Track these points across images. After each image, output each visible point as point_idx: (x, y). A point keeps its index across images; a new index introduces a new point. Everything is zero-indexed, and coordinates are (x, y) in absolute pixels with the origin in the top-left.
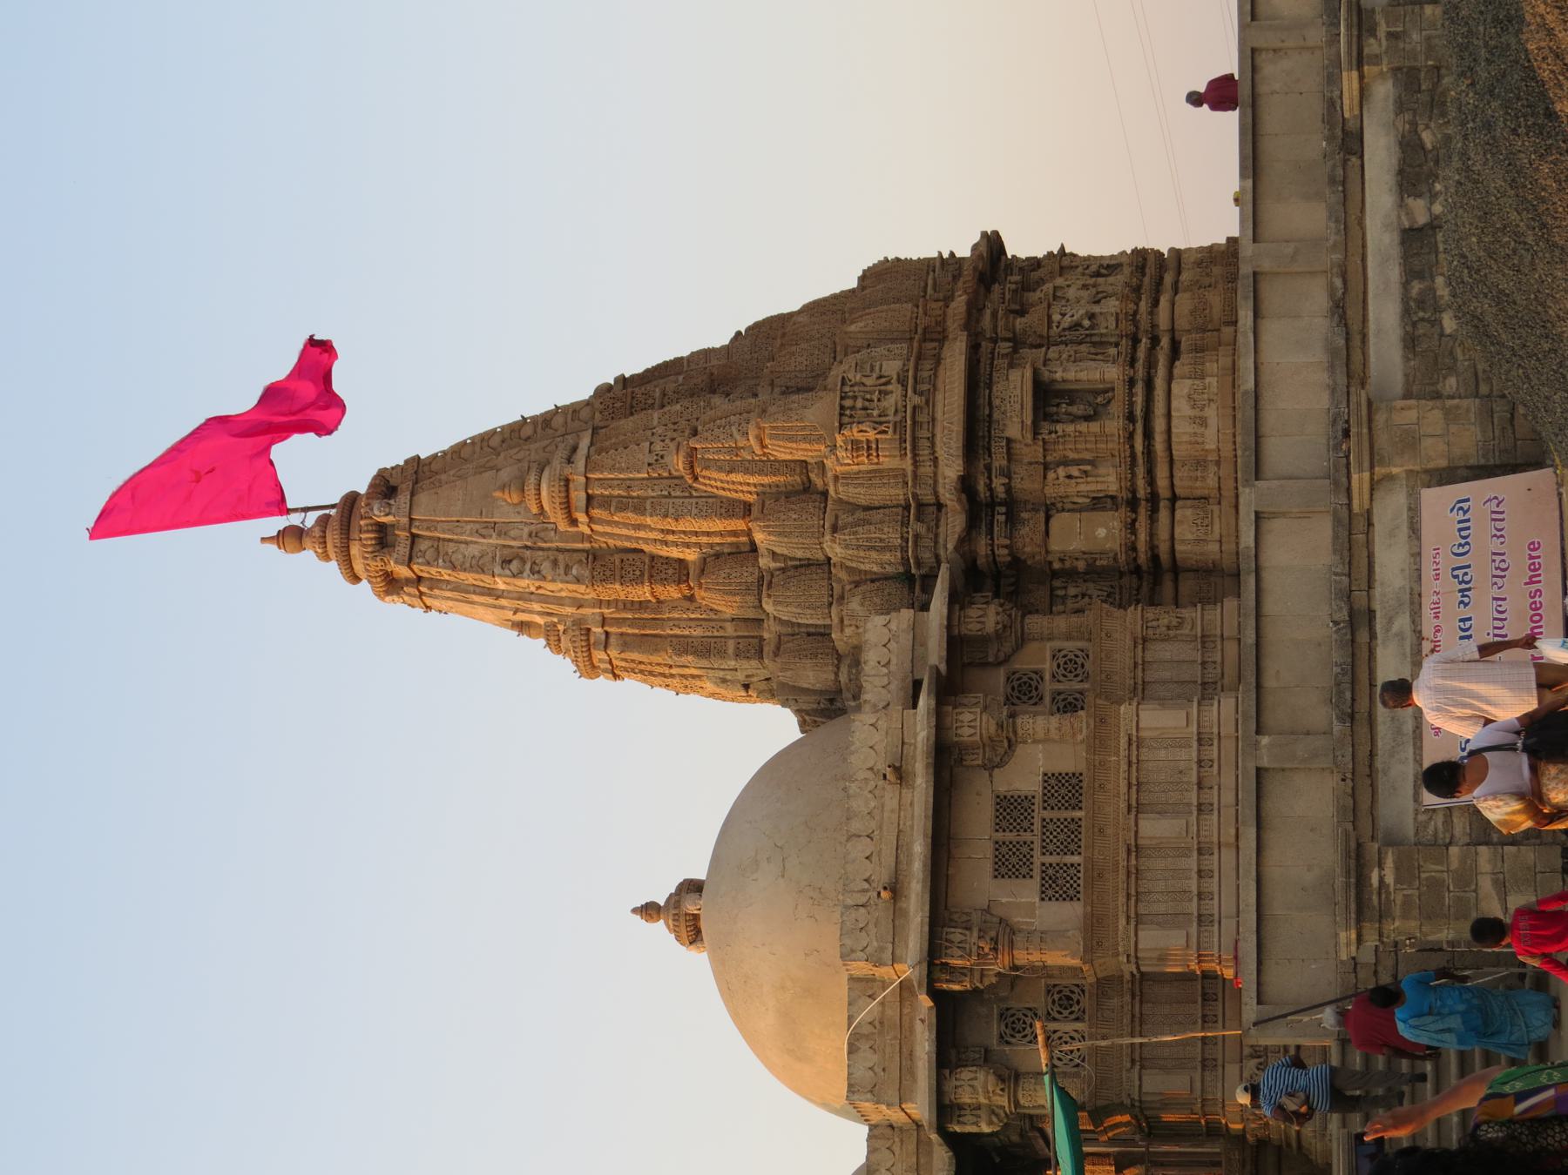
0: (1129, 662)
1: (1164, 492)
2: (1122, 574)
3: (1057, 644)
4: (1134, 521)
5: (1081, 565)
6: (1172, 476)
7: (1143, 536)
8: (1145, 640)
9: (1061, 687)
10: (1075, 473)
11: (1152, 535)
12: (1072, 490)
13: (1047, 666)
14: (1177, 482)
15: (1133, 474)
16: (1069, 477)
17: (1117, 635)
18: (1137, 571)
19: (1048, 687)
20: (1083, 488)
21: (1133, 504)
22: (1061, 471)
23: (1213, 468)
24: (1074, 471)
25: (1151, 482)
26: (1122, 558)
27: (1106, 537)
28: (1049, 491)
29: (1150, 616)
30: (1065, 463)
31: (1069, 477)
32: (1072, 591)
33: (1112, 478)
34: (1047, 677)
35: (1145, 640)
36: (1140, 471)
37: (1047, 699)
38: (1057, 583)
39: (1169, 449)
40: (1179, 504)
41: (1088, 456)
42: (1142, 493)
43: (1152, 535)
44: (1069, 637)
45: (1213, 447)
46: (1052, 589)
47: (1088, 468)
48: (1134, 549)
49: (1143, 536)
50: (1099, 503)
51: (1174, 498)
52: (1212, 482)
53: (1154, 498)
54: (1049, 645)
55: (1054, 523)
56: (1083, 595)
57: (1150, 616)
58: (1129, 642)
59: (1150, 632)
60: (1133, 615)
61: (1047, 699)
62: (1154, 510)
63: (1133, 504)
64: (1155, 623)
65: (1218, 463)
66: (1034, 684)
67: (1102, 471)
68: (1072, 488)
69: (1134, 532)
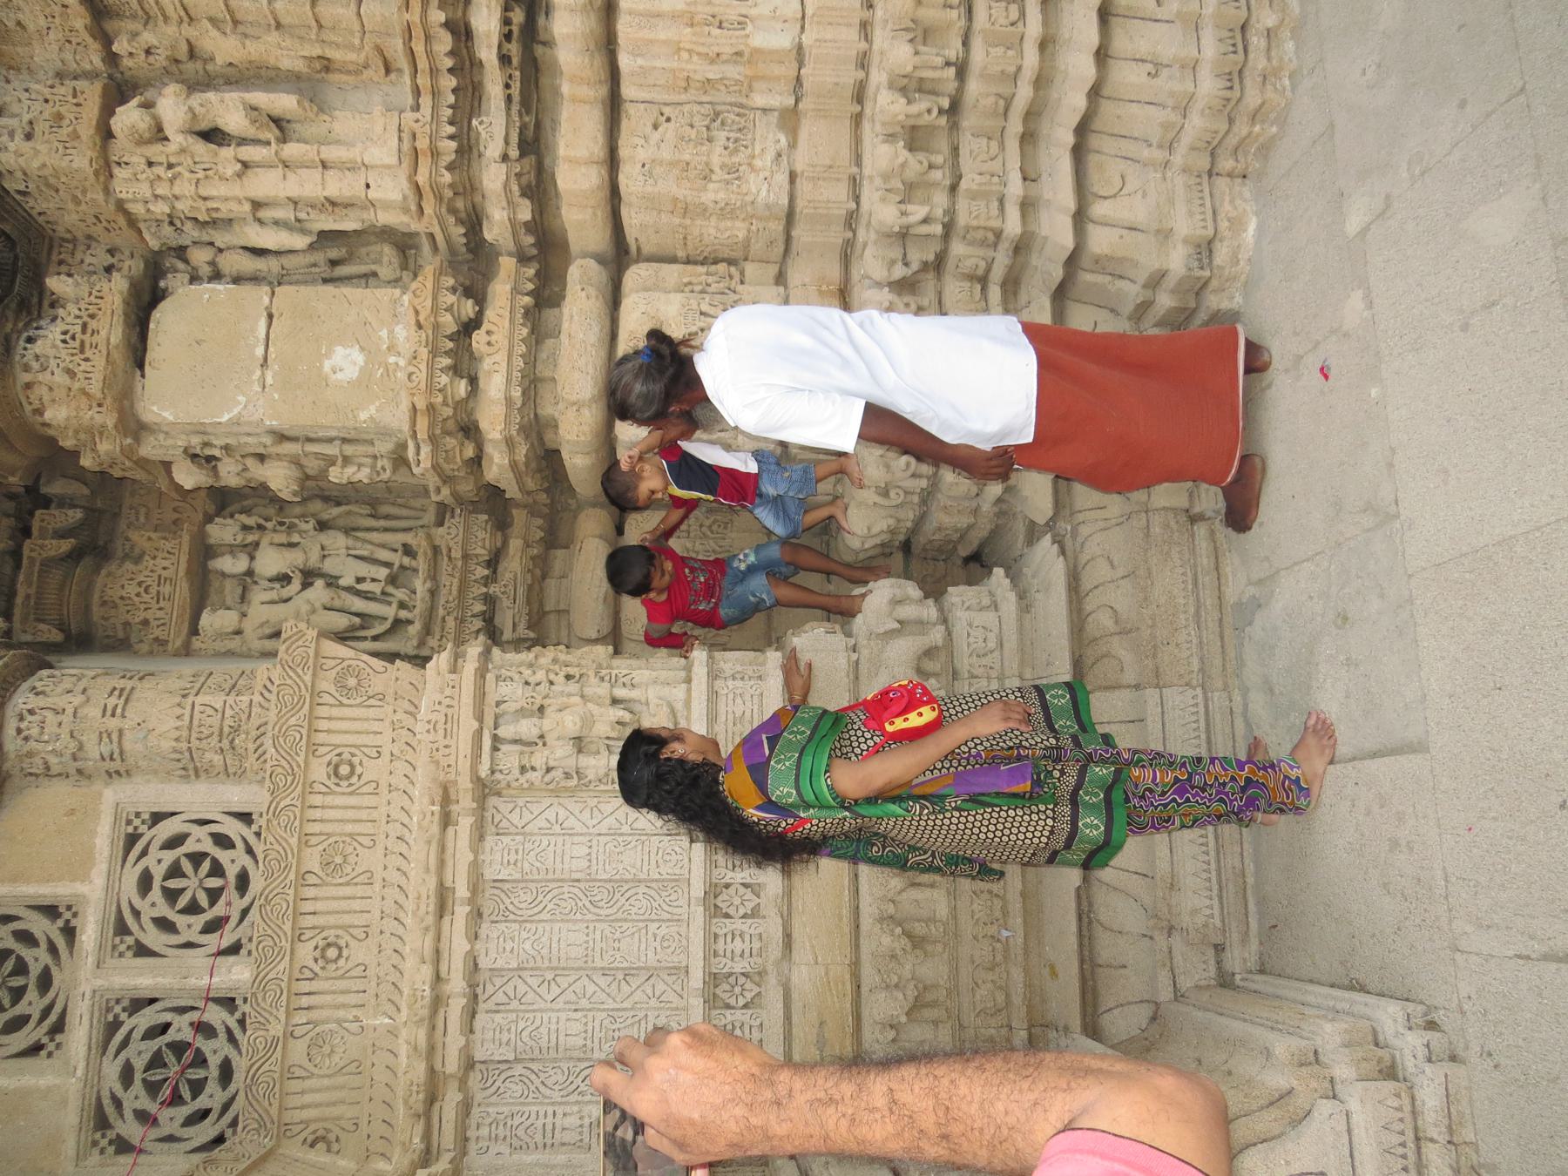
0: (422, 886)
1: (581, 222)
2: (443, 512)
3: (147, 794)
4: (469, 327)
5: (279, 478)
6: (612, 161)
7: (497, 383)
8: (485, 790)
9: (141, 977)
10: (229, 110)
11: (533, 383)
12: (227, 194)
13: (93, 890)
14: (629, 180)
15: (467, 149)
16: (213, 136)
17: (372, 770)
18: (493, 501)
19: (91, 977)
20: (266, 184)
21: (472, 265)
22: (172, 106)
23: (769, 139)
24: (229, 110)
25: (538, 187)
26: (422, 460)
27: (363, 382)
28: (131, 185)
29: (512, 693)
30: (199, 75)
31: (213, 136)
32: (270, 561)
33: (383, 152)
34: (89, 936)
35: (485, 790)
36: (495, 128)
37: (79, 1037)
38: (223, 531)
39: (608, 44)
40: (635, 276)
41: (289, 56)
42: (502, 220)
43: (533, 383)
44: (192, 770)
45: (780, 39)
46: (205, 552)
47: (284, 102)
48: (470, 430)
49: (497, 383)
50: (340, 253)
51: (619, 255)
52: (765, 188)
53: (546, 250)
54: (112, 796)
55: (165, 319)
56: (308, 576)
57: (512, 693)
58: (423, 807)
59: (510, 758)
60: (446, 684)
61: (79, 1037)
62: (545, 296)
63: (472, 265)
64: (527, 728)
65: (790, 120)
66: (37, 959)
67: (344, 123)
68: (221, 184)
69: (464, 365)
